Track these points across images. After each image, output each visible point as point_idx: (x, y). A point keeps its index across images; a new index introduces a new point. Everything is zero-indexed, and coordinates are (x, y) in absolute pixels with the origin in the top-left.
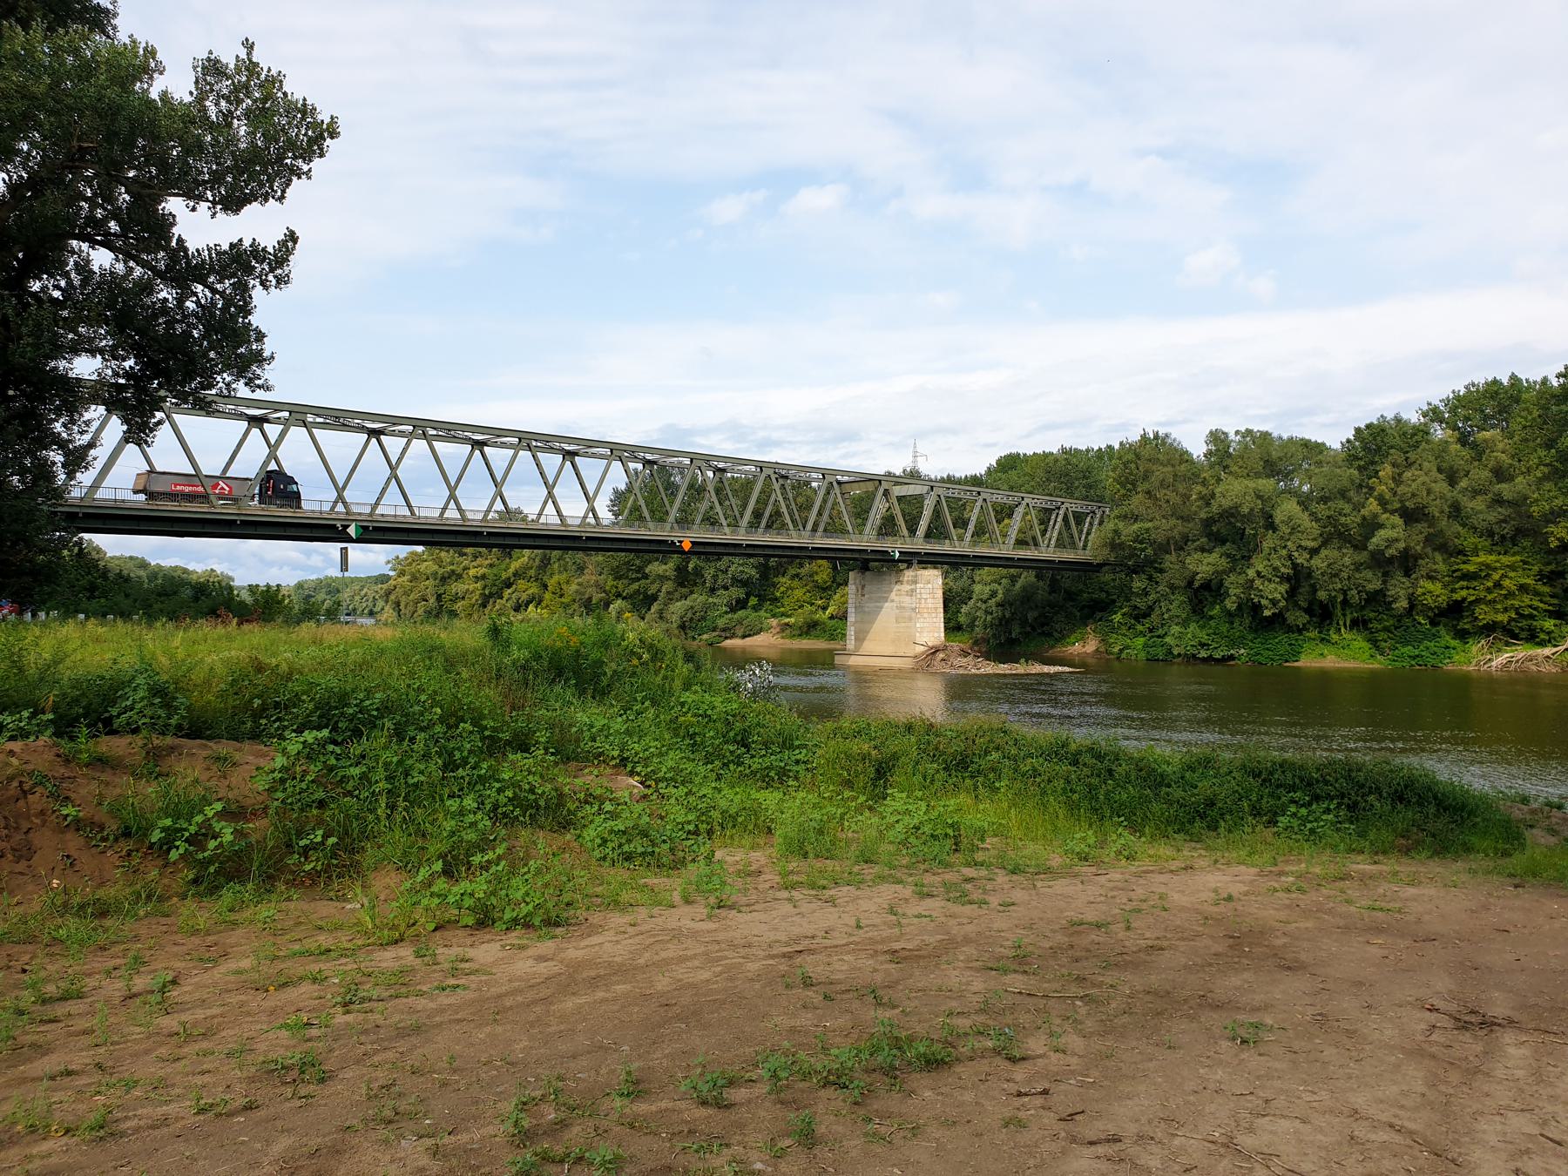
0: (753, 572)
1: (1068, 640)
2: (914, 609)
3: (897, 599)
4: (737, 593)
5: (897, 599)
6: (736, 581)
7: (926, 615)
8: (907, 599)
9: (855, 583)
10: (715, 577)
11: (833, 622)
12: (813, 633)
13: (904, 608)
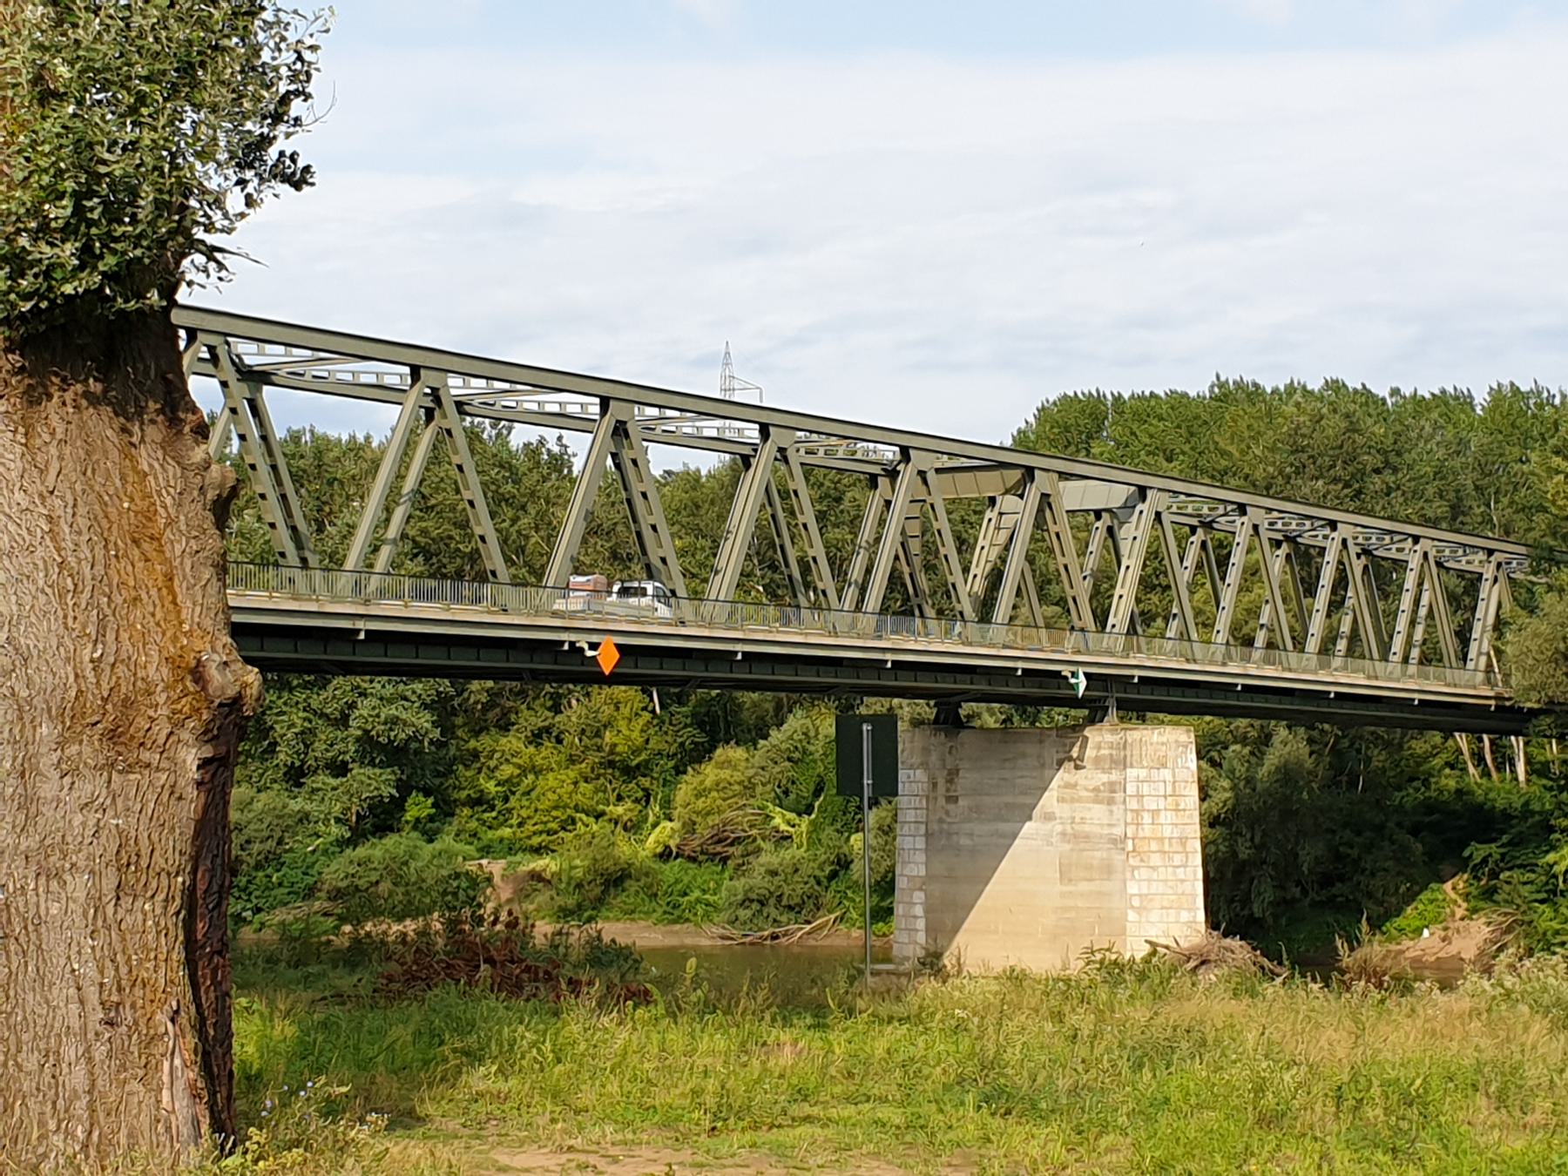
0: (425, 721)
1: (1399, 921)
2: (1118, 842)
3: (1063, 811)
4: (375, 781)
5: (1063, 811)
6: (373, 749)
7: (1156, 860)
8: (1098, 812)
9: (924, 765)
10: (307, 737)
11: (672, 870)
12: (618, 900)
13: (1087, 837)
